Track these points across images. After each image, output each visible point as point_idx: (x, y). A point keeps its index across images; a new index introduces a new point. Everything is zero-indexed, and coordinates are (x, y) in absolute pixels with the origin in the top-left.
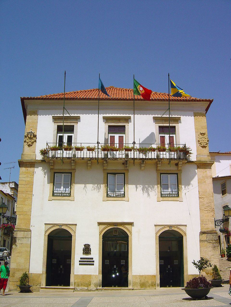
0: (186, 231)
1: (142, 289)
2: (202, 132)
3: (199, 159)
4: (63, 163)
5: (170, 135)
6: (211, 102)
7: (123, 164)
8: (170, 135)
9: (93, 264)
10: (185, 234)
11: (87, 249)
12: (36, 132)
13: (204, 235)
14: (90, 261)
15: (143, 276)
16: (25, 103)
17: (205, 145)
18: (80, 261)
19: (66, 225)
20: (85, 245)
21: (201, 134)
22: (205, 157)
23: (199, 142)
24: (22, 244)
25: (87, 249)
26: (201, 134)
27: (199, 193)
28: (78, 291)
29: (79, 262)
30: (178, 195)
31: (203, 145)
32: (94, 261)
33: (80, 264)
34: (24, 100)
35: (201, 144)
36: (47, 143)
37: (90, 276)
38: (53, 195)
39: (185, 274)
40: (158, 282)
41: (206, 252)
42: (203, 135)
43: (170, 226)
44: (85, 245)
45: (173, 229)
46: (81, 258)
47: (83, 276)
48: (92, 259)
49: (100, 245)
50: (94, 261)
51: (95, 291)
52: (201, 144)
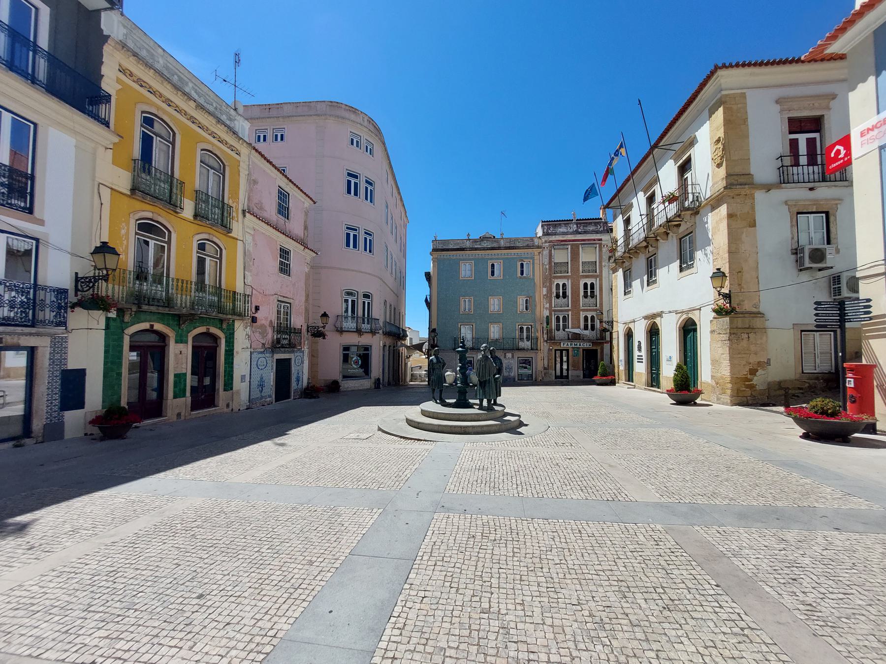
18: (638, 359)
38: (625, 295)
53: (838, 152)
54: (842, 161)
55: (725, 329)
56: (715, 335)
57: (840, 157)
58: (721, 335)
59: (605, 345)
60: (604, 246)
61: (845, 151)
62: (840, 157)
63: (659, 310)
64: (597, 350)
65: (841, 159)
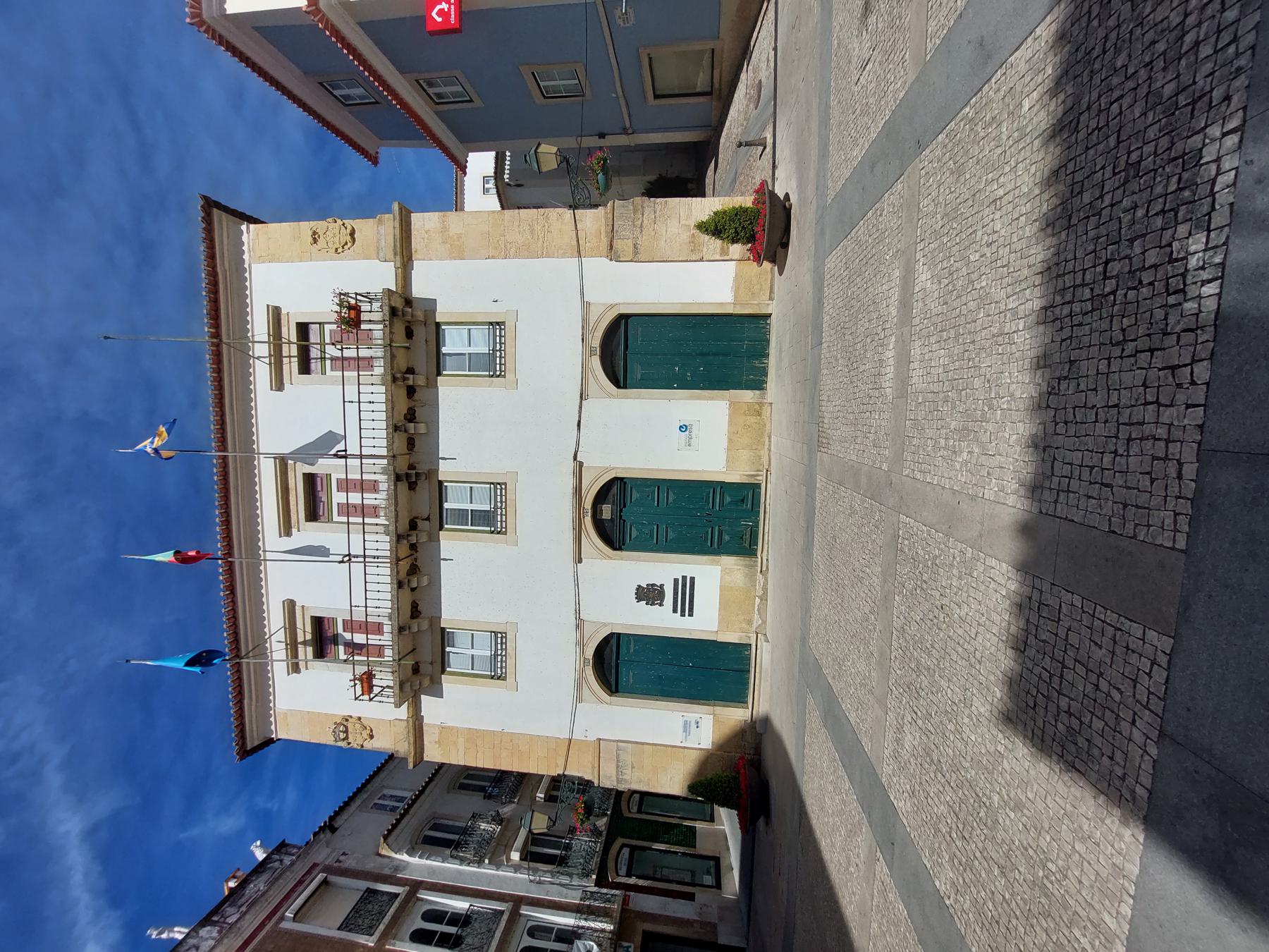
0: (604, 304)
1: (770, 445)
2: (310, 239)
3: (390, 255)
4: (414, 649)
5: (328, 344)
6: (210, 205)
7: (412, 486)
8: (328, 344)
9: (692, 579)
10: (612, 306)
11: (651, 595)
12: (335, 715)
13: (618, 244)
14: (684, 585)
15: (730, 440)
16: (256, 743)
17: (348, 231)
18: (683, 615)
19: (581, 644)
20: (639, 599)
21: (315, 241)
22: (382, 232)
23: (340, 250)
24: (632, 764)
25: (651, 595)
26: (315, 241)
27: (493, 257)
28: (764, 622)
29: (684, 616)
30: (498, 323)
31: (349, 238)
32: (684, 578)
33: (691, 614)
34: (248, 748)
35: (346, 243)
36: (356, 699)
37: (722, 588)
38: (505, 679)
39: (730, 310)
40: (748, 396)
41: (668, 241)
42: (319, 237)
43: (588, 352)
44: (639, 599)
45: (596, 343)
46: (675, 611)
47: (724, 605)
48: (676, 581)
49: (638, 560)
50: (684, 578)
51: (766, 580)
52: (346, 243)
53: (441, 13)
54: (452, 7)
55: (635, 211)
56: (643, 241)
57: (446, 10)
58: (645, 222)
59: (631, 906)
60: (338, 861)
61: (443, 3)
62: (446, 10)
63: (570, 465)
64: (645, 933)
65: (449, 9)
